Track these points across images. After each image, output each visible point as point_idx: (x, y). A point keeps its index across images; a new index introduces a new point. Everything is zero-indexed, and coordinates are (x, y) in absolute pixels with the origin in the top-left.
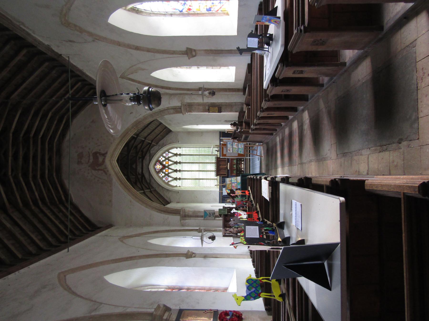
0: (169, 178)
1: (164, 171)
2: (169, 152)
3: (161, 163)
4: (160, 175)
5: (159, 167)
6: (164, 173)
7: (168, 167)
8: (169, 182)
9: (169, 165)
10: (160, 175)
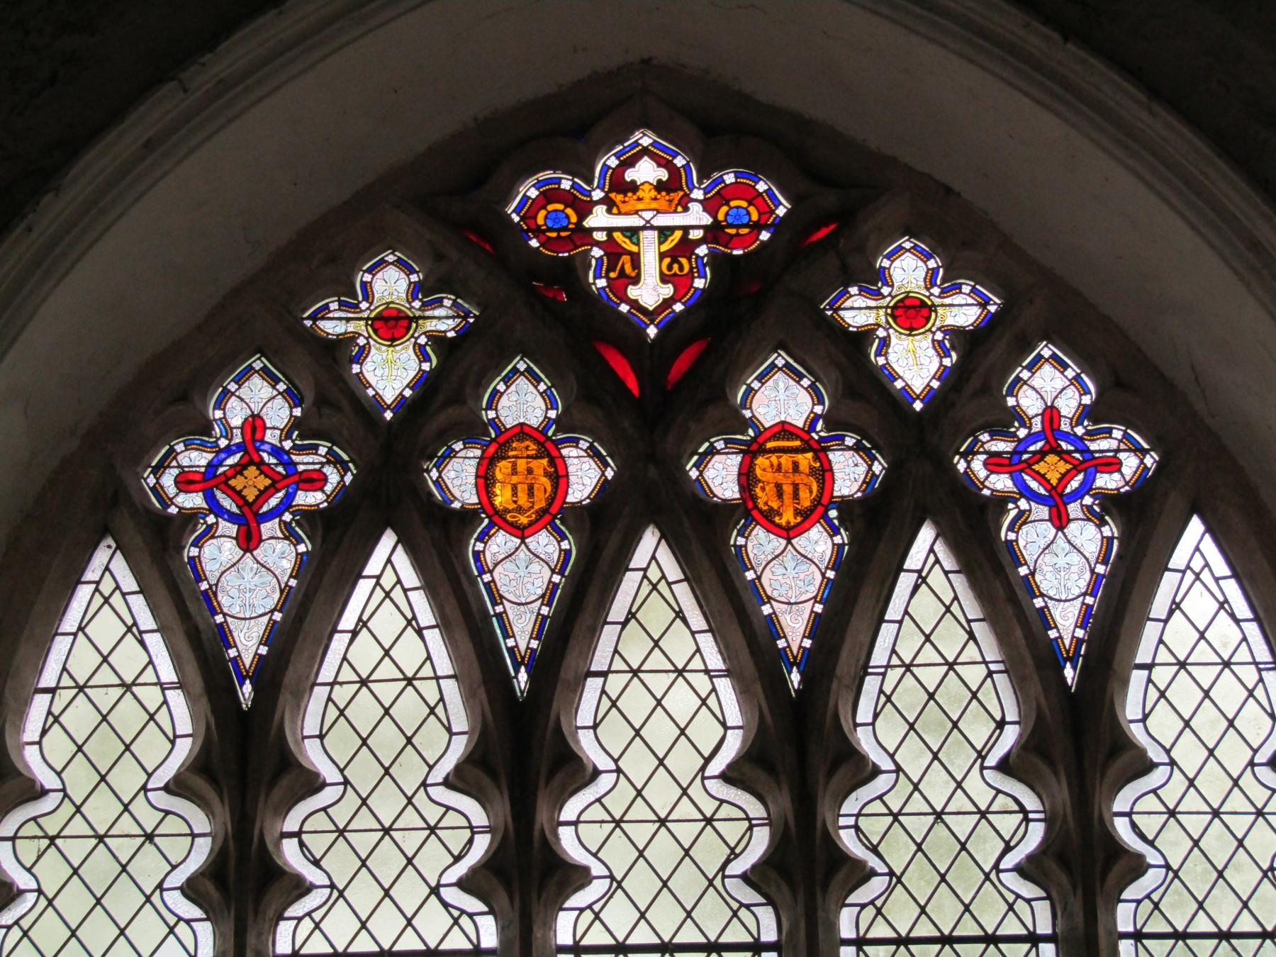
0: (281, 553)
1: (522, 402)
2: (1140, 530)
3: (759, 299)
4: (390, 285)
5: (649, 227)
6: (448, 401)
7: (654, 495)
8: (162, 551)
9: (707, 541)
10: (390, 285)
